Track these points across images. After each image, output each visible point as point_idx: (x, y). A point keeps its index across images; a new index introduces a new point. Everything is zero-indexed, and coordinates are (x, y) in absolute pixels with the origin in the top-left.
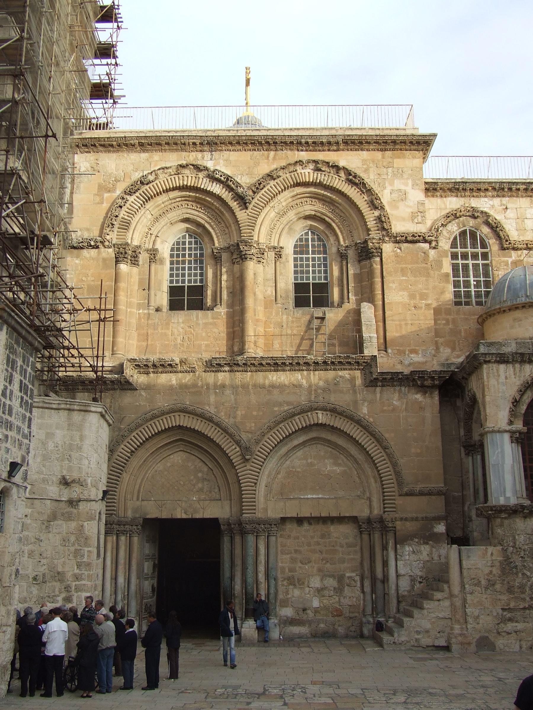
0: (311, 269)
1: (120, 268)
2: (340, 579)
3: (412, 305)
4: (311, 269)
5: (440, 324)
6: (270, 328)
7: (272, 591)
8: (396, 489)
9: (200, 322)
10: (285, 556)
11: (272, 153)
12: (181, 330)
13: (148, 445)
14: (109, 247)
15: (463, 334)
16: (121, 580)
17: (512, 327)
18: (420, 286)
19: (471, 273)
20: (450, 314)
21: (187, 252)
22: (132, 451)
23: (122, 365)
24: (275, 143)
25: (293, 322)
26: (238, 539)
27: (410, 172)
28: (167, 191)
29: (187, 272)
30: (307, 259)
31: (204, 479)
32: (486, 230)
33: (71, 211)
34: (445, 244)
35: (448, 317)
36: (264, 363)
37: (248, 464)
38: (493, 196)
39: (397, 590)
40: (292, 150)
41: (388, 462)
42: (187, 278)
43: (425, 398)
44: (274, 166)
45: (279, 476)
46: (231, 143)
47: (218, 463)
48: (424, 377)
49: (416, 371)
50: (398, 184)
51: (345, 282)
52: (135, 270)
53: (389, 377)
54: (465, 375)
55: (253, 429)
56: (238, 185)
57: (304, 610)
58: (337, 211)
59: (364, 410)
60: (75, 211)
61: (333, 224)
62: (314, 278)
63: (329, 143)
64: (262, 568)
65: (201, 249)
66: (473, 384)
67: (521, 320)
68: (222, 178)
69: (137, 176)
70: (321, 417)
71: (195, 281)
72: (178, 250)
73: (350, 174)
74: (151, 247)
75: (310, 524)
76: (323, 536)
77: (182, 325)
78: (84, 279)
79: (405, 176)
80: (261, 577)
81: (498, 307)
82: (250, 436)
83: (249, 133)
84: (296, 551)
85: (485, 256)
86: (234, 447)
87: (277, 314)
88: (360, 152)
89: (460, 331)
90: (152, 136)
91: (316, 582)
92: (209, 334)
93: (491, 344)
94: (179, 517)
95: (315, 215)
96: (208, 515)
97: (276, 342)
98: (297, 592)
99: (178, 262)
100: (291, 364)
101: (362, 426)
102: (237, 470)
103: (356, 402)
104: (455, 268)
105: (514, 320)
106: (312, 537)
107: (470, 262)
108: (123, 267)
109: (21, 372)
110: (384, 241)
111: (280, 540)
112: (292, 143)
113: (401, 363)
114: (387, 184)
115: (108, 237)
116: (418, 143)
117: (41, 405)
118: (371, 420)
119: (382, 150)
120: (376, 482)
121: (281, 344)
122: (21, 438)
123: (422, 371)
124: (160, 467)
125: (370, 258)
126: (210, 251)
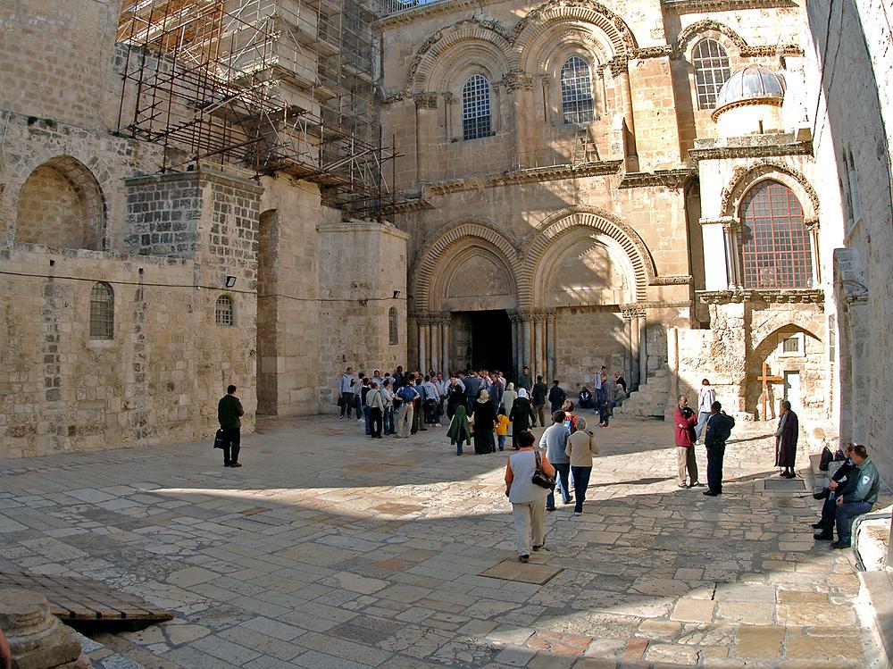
2: (608, 359)
5: (687, 127)
7: (551, 369)
10: (561, 340)
13: (448, 252)
14: (410, 98)
16: (435, 360)
21: (476, 90)
26: (519, 325)
29: (476, 107)
31: (495, 278)
32: (724, 38)
33: (382, 76)
36: (530, 175)
37: (521, 263)
39: (647, 368)
42: (477, 112)
52: (433, 111)
56: (503, 29)
57: (578, 385)
59: (617, 211)
60: (385, 74)
64: (539, 350)
65: (487, 86)
69: (427, 37)
72: (469, 89)
74: (445, 91)
75: (582, 312)
76: (593, 323)
80: (539, 358)
84: (571, 336)
85: (726, 63)
87: (547, 132)
91: (587, 362)
93: (704, 141)
94: (476, 310)
95: (574, 43)
96: (498, 308)
98: (572, 370)
99: (469, 100)
103: (611, 203)
106: (585, 324)
108: (422, 111)
111: (557, 326)
117: (333, 230)
124: (461, 269)
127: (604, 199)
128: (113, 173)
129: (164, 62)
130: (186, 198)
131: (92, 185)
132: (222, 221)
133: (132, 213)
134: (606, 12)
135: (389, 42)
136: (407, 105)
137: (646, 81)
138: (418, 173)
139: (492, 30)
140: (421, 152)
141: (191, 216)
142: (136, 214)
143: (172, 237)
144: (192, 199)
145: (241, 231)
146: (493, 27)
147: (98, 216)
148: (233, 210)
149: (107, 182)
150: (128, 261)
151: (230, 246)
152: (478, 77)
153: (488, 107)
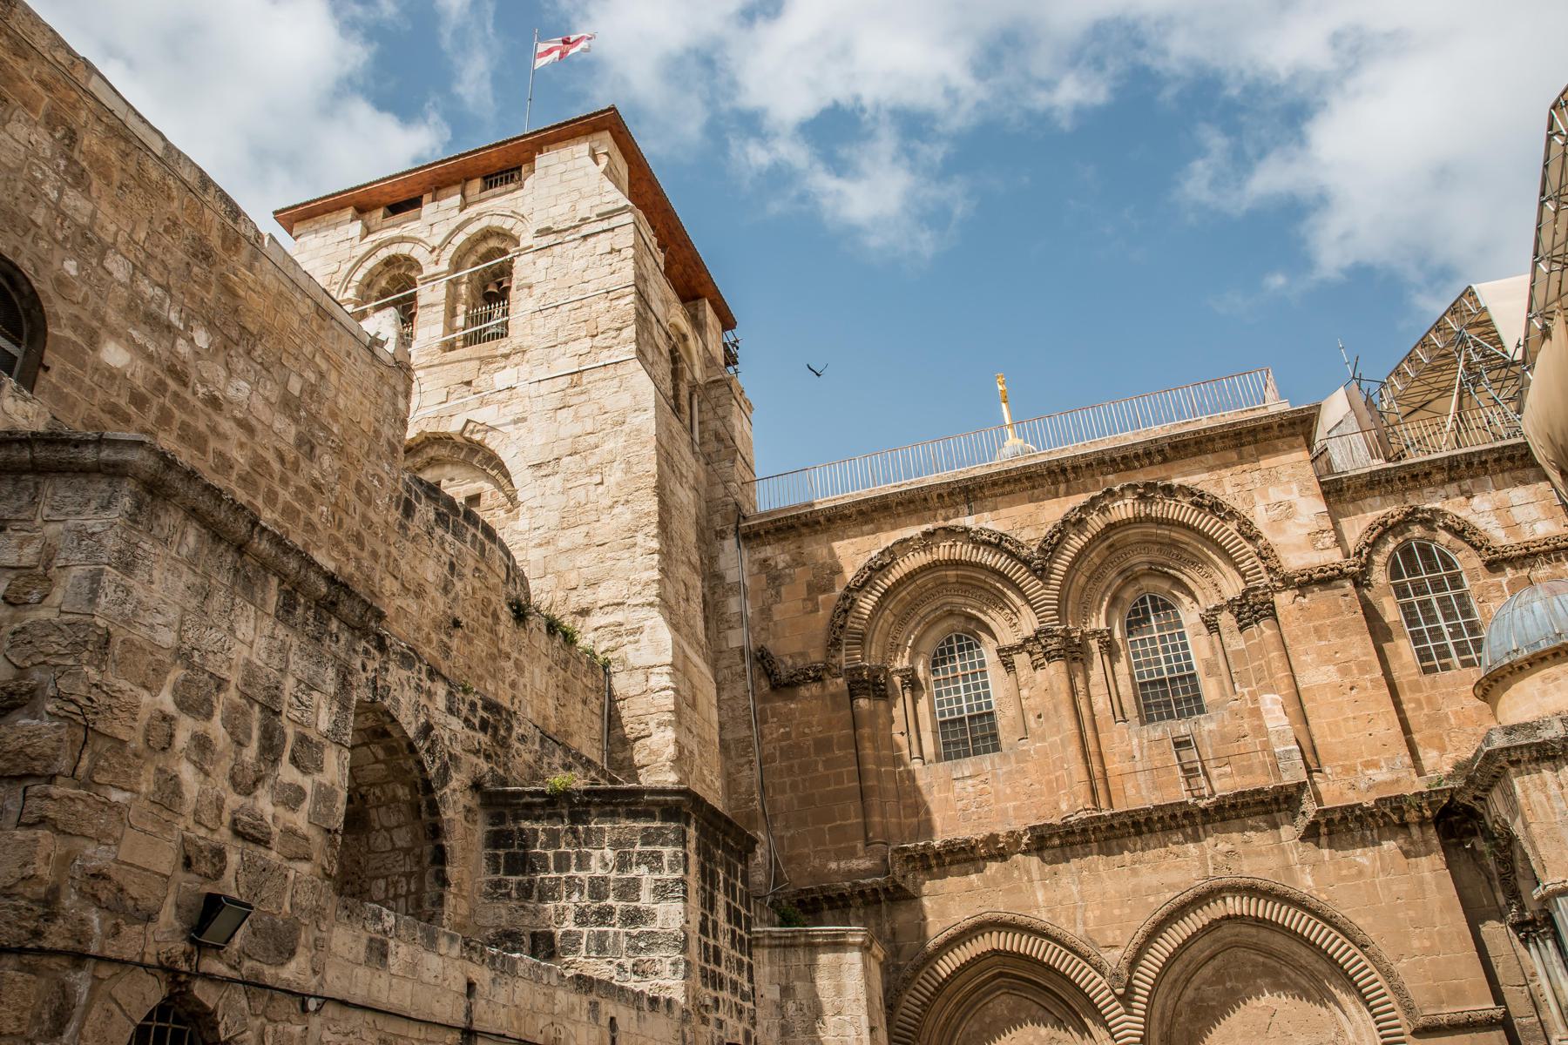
0: (1161, 656)
1: (858, 706)
3: (1349, 686)
4: (1161, 656)
6: (1114, 763)
8: (1402, 1019)
9: (1000, 772)
11: (1062, 487)
12: (970, 789)
15: (1453, 721)
17: (1544, 693)
18: (1354, 651)
19: (1439, 615)
20: (1421, 691)
22: (923, 1003)
23: (885, 860)
24: (1064, 471)
25: (1150, 748)
27: (1291, 471)
28: (911, 576)
29: (963, 694)
30: (1152, 640)
34: (1379, 576)
35: (1417, 695)
36: (1116, 823)
38: (1443, 483)
40: (1093, 476)
41: (1374, 970)
42: (964, 704)
43: (1412, 843)
44: (1071, 506)
45: (1181, 1019)
46: (994, 484)
47: (1070, 1007)
48: (1401, 808)
49: (1386, 799)
50: (1275, 494)
51: (1223, 666)
53: (1337, 816)
54: (1478, 793)
55: (1119, 939)
56: (1020, 545)
58: (1185, 556)
59: (1305, 884)
61: (1185, 579)
62: (1170, 670)
63: (1148, 454)
66: (1497, 804)
67: (1557, 679)
68: (992, 539)
70: (1234, 905)
71: (979, 707)
73: (1193, 494)
77: (970, 782)
78: (807, 731)
79: (1284, 479)
81: (1506, 661)
82: (1118, 953)
83: (1020, 464)
85: (1456, 581)
86: (1091, 975)
88: (1202, 458)
89: (1447, 717)
90: (875, 498)
92: (1017, 789)
97: (1129, 786)
100: (1161, 818)
101: (1309, 910)
102: (1104, 1016)
103: (1288, 868)
104: (1407, 610)
105: (1544, 680)
107: (1433, 597)
108: (863, 703)
109: (726, 891)
110: (1276, 590)
112: (1089, 465)
113: (1353, 787)
114: (1256, 498)
115: (834, 661)
116: (1292, 423)
117: (767, 942)
118: (1323, 896)
119: (1236, 446)
120: (1360, 1011)
121: (1138, 787)
122: (740, 1002)
123: (1396, 797)
125: (1256, 621)
126: (995, 657)
127: (1273, 862)
128: (458, 769)
129: (480, 536)
130: (650, 848)
131: (402, 792)
132: (712, 908)
133: (501, 875)
134: (1215, 507)
135: (781, 565)
136: (832, 689)
137: (1316, 630)
138: (866, 827)
139: (998, 546)
140: (870, 783)
141: (662, 891)
142: (513, 878)
143: (615, 944)
144: (667, 851)
145: (733, 932)
146: (998, 544)
147: (408, 876)
148: (721, 884)
149: (446, 790)
150: (593, 997)
151: (722, 970)
152: (959, 638)
153: (987, 695)
